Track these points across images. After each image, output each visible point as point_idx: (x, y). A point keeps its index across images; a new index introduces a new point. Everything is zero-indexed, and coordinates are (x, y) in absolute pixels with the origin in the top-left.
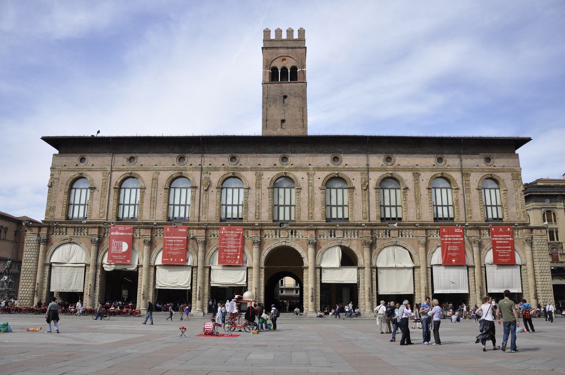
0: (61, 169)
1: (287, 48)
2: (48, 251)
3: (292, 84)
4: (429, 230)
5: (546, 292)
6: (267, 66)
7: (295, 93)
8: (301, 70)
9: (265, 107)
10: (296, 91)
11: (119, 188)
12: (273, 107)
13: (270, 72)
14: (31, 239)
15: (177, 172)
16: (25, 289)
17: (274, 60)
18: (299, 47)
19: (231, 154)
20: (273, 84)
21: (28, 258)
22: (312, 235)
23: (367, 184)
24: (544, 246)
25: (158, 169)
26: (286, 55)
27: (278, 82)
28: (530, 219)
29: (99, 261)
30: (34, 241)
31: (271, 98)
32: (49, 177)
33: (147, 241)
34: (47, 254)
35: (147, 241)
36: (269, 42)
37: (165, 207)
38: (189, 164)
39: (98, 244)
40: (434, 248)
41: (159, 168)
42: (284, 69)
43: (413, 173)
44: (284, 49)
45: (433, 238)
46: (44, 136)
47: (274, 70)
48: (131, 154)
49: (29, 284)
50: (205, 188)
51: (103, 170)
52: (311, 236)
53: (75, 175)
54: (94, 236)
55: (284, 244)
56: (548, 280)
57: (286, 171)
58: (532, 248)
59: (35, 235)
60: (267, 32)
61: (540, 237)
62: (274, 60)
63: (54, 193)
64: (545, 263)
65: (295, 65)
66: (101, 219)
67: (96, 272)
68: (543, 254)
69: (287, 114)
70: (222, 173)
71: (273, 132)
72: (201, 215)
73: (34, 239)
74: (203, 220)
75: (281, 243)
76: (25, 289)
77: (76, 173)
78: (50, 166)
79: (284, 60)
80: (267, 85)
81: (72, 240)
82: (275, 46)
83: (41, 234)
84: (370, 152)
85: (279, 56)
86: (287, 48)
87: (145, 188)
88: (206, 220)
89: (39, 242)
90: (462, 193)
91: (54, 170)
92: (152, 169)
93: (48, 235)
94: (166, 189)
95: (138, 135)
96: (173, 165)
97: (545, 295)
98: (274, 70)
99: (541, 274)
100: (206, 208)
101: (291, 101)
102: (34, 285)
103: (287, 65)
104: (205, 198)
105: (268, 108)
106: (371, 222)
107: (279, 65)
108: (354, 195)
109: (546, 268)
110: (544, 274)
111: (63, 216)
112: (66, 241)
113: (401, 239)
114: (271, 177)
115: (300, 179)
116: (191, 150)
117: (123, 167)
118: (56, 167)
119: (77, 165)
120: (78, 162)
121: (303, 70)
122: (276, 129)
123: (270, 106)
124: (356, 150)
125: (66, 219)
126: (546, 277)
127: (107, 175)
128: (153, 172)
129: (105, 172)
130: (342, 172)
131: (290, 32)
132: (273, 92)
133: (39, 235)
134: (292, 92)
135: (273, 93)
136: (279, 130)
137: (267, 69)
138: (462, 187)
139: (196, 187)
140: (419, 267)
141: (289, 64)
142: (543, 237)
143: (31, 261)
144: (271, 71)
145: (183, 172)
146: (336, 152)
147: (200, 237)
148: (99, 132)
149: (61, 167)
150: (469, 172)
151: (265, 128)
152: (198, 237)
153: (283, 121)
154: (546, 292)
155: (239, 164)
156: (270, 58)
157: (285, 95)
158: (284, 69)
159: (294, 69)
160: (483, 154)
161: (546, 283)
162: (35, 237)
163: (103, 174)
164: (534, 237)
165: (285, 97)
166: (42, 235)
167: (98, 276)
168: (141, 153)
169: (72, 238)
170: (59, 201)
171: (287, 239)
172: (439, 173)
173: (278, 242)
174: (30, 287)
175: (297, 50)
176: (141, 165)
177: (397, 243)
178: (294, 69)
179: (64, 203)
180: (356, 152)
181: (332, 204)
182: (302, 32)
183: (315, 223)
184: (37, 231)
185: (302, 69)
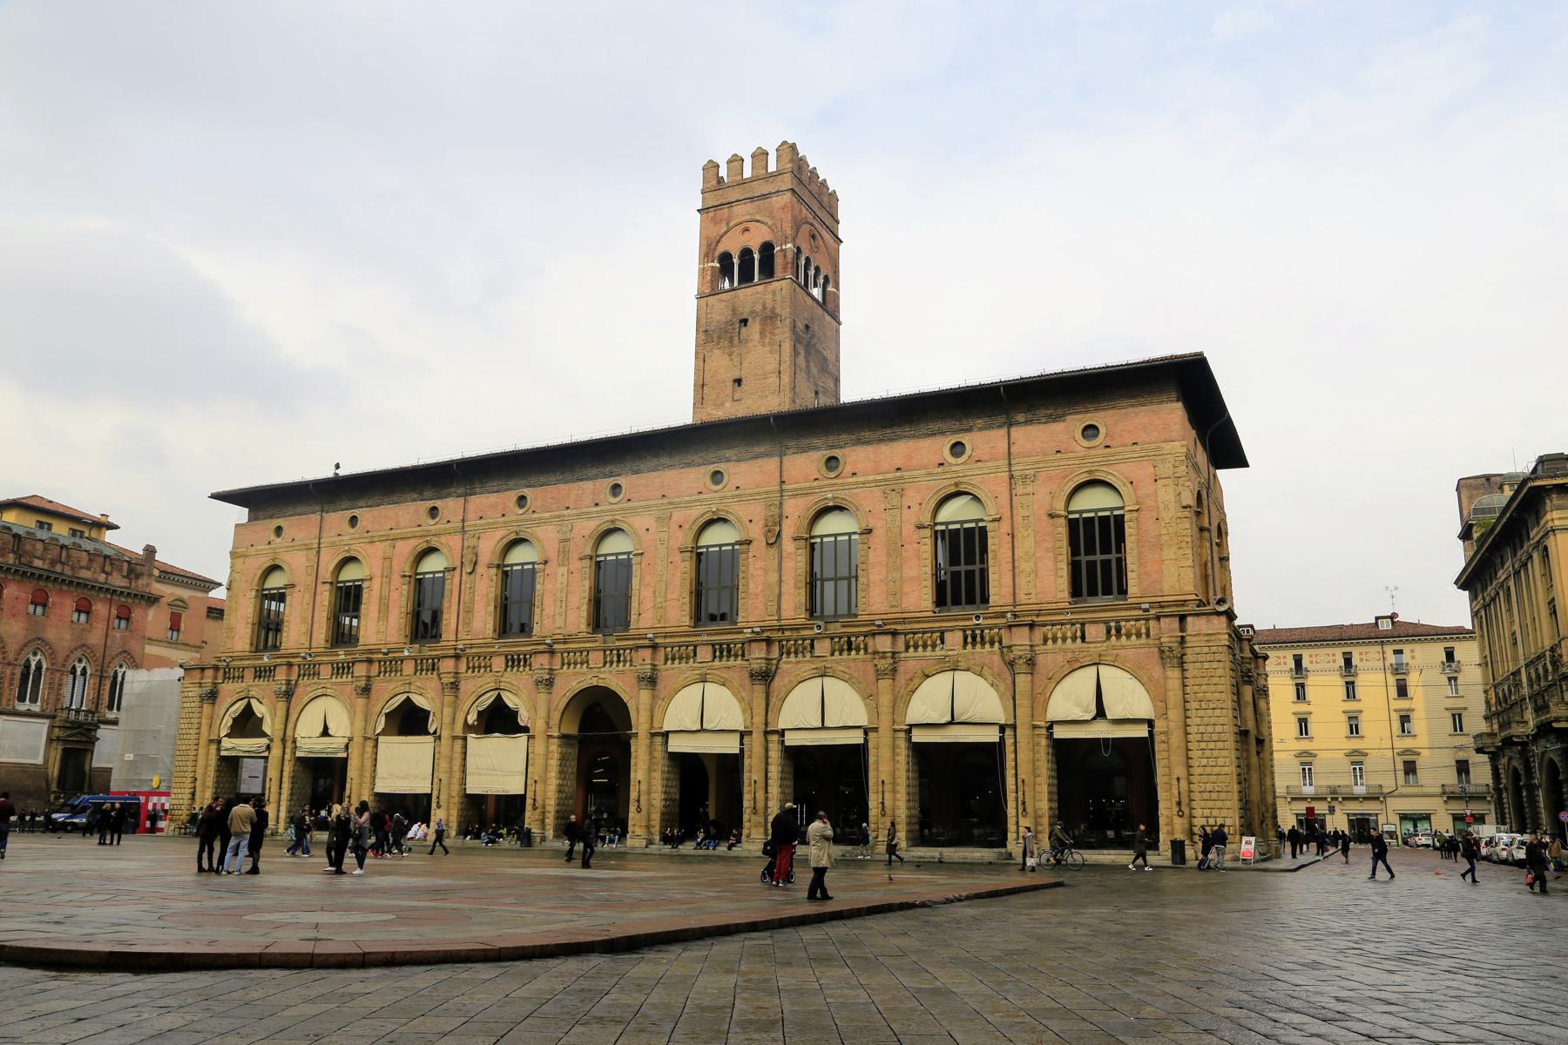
1: (751, 199)
3: (760, 288)
4: (902, 633)
5: (1214, 795)
6: (706, 255)
8: (779, 248)
9: (701, 356)
11: (331, 583)
13: (713, 267)
17: (722, 237)
18: (778, 192)
19: (516, 492)
23: (778, 529)
24: (1215, 665)
26: (748, 217)
28: (1043, 601)
29: (289, 733)
32: (229, 570)
38: (445, 521)
40: (916, 681)
45: (916, 654)
46: (215, 491)
47: (726, 259)
48: (612, 479)
50: (469, 571)
52: (642, 662)
55: (595, 682)
56: (1221, 762)
57: (617, 517)
58: (1184, 670)
60: (712, 166)
61: (1206, 638)
64: (1218, 712)
65: (768, 237)
67: (284, 754)
68: (1213, 688)
69: (745, 365)
71: (715, 412)
72: (460, 628)
74: (465, 637)
78: (230, 548)
79: (747, 230)
82: (727, 201)
84: (792, 450)
86: (751, 199)
87: (371, 579)
88: (469, 637)
90: (1010, 531)
93: (215, 684)
94: (404, 576)
95: (421, 463)
97: (1210, 804)
98: (726, 259)
99: (1203, 745)
100: (469, 611)
104: (468, 591)
106: (783, 622)
107: (733, 244)
109: (1219, 729)
110: (1212, 745)
113: (837, 662)
114: (587, 533)
120: (273, 537)
121: (784, 247)
122: (722, 404)
125: (253, 649)
126: (1216, 753)
128: (384, 544)
135: (718, 318)
136: (728, 405)
138: (1009, 513)
139: (454, 569)
142: (1213, 638)
144: (718, 265)
145: (434, 538)
146: (720, 460)
148: (337, 466)
151: (700, 406)
153: (738, 381)
154: (1214, 795)
155: (530, 511)
156: (715, 232)
158: (746, 253)
159: (767, 248)
160: (1075, 417)
161: (1216, 770)
163: (307, 556)
164: (1188, 638)
165: (744, 322)
167: (286, 763)
171: (603, 670)
172: (950, 485)
177: (828, 670)
178: (767, 248)
183: (667, 630)
184: (199, 676)
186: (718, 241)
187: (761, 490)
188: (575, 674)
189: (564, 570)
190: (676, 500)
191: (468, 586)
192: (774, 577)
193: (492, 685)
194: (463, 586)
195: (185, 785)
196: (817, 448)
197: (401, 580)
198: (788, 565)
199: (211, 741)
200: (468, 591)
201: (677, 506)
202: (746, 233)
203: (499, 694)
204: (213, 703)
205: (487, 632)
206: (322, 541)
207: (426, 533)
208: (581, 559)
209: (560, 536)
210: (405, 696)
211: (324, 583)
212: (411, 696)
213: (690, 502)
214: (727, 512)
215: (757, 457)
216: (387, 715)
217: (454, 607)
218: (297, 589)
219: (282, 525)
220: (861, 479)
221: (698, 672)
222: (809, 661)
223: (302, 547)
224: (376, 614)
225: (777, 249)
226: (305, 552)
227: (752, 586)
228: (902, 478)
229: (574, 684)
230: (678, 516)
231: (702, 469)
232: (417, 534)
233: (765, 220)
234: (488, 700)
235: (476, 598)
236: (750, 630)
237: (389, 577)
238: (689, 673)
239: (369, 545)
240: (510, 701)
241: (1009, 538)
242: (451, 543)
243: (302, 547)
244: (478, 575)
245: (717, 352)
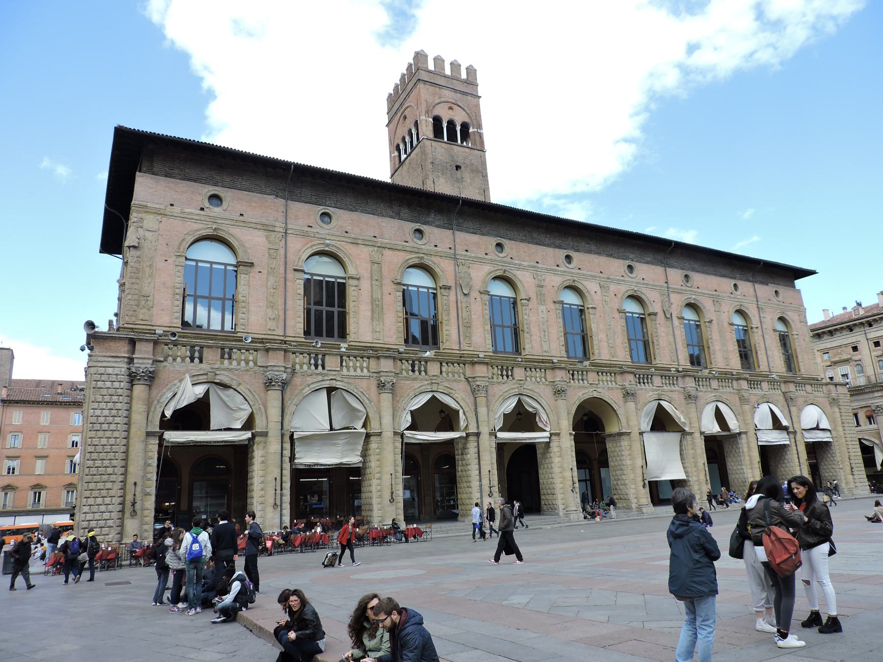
0: (162, 212)
1: (455, 91)
2: (155, 402)
7: (472, 165)
8: (476, 130)
10: (473, 162)
14: (110, 370)
15: (414, 256)
16: (99, 501)
17: (436, 105)
20: (437, 143)
21: (102, 420)
22: (631, 381)
25: (379, 245)
26: (453, 101)
27: (442, 141)
30: (117, 375)
31: (438, 165)
33: (389, 382)
34: (153, 409)
35: (389, 382)
36: (428, 73)
37: (401, 319)
39: (283, 387)
41: (381, 243)
42: (451, 123)
43: (713, 301)
44: (451, 91)
47: (437, 121)
49: (109, 485)
51: (267, 228)
53: (200, 230)
54: (276, 368)
55: (595, 395)
57: (575, 279)
59: (119, 360)
62: (436, 105)
63: (148, 263)
65: (467, 120)
66: (270, 333)
70: (487, 268)
72: (461, 339)
73: (117, 371)
74: (467, 348)
75: (592, 394)
76: (99, 501)
77: (201, 226)
79: (451, 108)
80: (430, 141)
81: (218, 377)
83: (136, 358)
85: (443, 100)
86: (455, 91)
89: (132, 378)
91: (144, 210)
92: (370, 244)
96: (405, 241)
100: (468, 327)
101: (466, 174)
102: (123, 488)
103: (455, 118)
104: (464, 310)
108: (658, 326)
111: (175, 321)
112: (201, 377)
114: (557, 285)
115: (593, 293)
116: (430, 219)
117: (309, 229)
118: (149, 205)
119: (202, 209)
120: (207, 204)
121: (479, 130)
123: (438, 177)
124: (649, 259)
127: (277, 241)
128: (371, 249)
129: (273, 234)
130: (644, 290)
131: (455, 66)
132: (441, 156)
133: (131, 360)
134: (467, 162)
135: (440, 157)
137: (428, 117)
140: (746, 433)
141: (459, 118)
143: (113, 427)
145: (426, 257)
147: (481, 379)
149: (162, 207)
150: (763, 307)
152: (478, 379)
157: (458, 164)
159: (465, 127)
162: (122, 368)
166: (141, 361)
168: (341, 209)
169: (218, 372)
170: (164, 284)
173: (587, 391)
174: (112, 493)
175: (469, 97)
176: (346, 232)
179: (177, 291)
180: (649, 262)
182: (471, 71)
186: (434, 107)
187: (658, 284)
188: (580, 387)
189: (542, 308)
190: (611, 277)
191: (464, 305)
192: (672, 339)
193: (516, 391)
194: (459, 305)
195: (112, 493)
197: (394, 286)
198: (677, 332)
199: (149, 434)
200: (464, 310)
201: (612, 281)
202: (450, 111)
203: (519, 401)
204: (150, 386)
205: (488, 346)
206: (290, 226)
207: (416, 250)
208: (554, 302)
209: (537, 282)
210: (429, 396)
211: (295, 270)
212: (436, 395)
213: (618, 280)
214: (642, 293)
216: (412, 413)
217: (453, 319)
218: (256, 269)
219: (221, 195)
220: (703, 291)
221: (657, 393)
222: (710, 391)
223: (259, 226)
224: (369, 314)
225: (471, 130)
226: (261, 233)
227: (661, 342)
228: (719, 296)
229: (580, 394)
230: (613, 288)
231: (621, 261)
232: (407, 249)
233: (465, 108)
234: (510, 405)
235: (473, 317)
236: (674, 369)
237: (380, 280)
238: (651, 393)
239: (351, 246)
240: (530, 405)
241: (762, 337)
242: (442, 265)
243: (259, 226)
244: (473, 300)
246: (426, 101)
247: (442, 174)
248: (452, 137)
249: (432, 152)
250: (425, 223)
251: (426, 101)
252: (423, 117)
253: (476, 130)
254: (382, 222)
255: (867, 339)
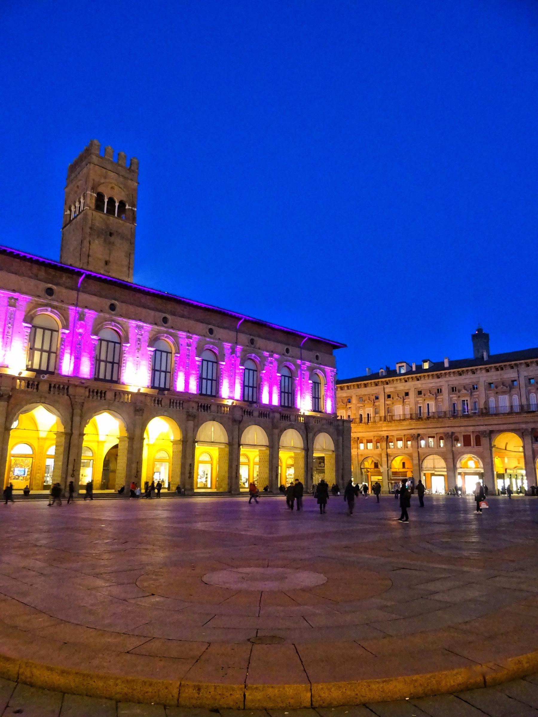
12: (96, 242)
105: (92, 241)
116: (61, 281)
121: (133, 208)
123: (94, 240)
134: (120, 231)
137: (93, 192)
181: (203, 377)
185: (132, 207)
196: (246, 334)
215: (225, 328)
245: (96, 242)
246: (94, 180)
247: (98, 237)
248: (111, 211)
249: (92, 220)
250: (57, 284)
251: (94, 180)
252: (89, 192)
253: (130, 208)
254: (22, 280)
255: (384, 392)
